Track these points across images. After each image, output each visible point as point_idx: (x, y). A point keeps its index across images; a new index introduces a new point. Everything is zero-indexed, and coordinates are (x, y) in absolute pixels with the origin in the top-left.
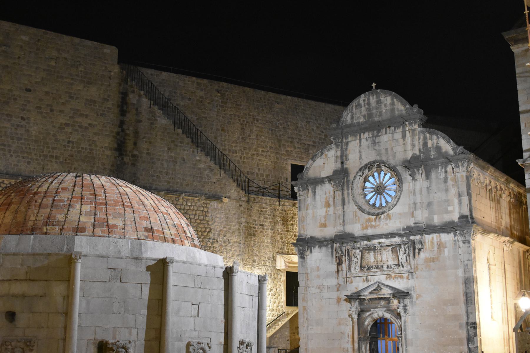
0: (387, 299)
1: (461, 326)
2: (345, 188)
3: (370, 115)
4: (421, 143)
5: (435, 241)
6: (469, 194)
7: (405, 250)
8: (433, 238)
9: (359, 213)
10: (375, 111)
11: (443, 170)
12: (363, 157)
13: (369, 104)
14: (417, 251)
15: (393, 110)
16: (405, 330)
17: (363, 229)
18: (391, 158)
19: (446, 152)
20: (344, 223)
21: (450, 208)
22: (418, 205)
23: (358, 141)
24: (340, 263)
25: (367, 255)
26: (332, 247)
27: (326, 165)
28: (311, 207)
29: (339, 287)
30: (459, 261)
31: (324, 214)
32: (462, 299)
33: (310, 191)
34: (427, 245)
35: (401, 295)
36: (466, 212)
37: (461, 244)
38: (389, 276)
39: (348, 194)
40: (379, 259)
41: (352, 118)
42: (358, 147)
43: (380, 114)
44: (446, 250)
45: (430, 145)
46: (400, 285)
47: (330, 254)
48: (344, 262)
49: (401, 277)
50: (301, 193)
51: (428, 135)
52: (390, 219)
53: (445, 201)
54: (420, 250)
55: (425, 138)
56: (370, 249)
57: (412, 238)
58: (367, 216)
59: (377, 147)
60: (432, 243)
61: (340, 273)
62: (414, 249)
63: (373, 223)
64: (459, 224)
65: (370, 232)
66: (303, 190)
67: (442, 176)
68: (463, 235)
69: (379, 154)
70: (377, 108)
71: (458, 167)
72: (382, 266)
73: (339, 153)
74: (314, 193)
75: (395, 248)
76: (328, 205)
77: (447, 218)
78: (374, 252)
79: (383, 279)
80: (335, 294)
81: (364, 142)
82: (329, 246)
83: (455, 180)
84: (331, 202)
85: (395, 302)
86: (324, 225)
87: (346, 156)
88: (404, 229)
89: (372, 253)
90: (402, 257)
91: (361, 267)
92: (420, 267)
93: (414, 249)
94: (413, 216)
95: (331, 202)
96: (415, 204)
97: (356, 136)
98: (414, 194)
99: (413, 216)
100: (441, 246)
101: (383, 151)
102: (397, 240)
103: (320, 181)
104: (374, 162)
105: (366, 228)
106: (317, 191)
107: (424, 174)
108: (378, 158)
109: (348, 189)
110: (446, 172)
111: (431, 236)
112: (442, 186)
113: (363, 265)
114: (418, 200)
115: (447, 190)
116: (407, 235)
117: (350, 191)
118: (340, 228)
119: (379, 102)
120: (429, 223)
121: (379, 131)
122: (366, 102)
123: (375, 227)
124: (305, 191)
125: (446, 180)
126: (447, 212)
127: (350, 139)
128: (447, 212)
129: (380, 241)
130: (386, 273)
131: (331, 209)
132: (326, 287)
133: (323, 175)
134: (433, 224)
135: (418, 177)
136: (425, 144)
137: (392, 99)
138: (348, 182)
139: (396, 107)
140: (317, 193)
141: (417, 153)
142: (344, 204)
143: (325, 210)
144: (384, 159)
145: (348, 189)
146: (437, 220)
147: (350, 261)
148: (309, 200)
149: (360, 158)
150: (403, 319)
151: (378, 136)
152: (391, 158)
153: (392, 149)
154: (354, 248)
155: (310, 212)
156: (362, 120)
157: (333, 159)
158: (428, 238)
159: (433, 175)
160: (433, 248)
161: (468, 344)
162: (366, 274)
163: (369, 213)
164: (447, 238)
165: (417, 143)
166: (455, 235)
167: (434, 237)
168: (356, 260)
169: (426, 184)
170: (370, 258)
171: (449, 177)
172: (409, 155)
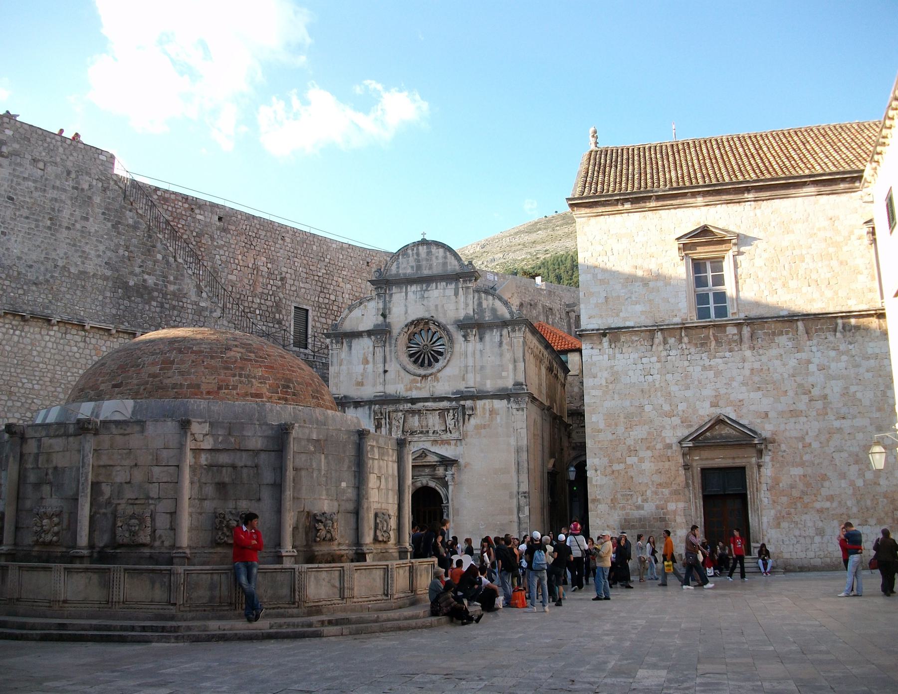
0: (433, 467)
1: (511, 497)
2: (387, 344)
3: (419, 267)
4: (476, 303)
5: (487, 407)
6: (524, 360)
7: (454, 415)
8: (485, 404)
9: (403, 373)
10: (424, 263)
11: (498, 333)
12: (409, 311)
13: (418, 254)
14: (467, 417)
15: (445, 264)
16: (452, 500)
17: (407, 390)
18: (441, 315)
19: (502, 315)
20: (384, 383)
21: (504, 374)
22: (470, 368)
23: (404, 294)
25: (411, 419)
26: (370, 408)
28: (345, 362)
30: (512, 429)
31: (361, 371)
32: (513, 468)
33: (345, 344)
34: (479, 411)
35: (447, 462)
36: (521, 379)
37: (515, 411)
38: (435, 442)
39: (391, 351)
40: (424, 423)
41: (398, 268)
42: (404, 301)
43: (431, 268)
44: (498, 418)
45: (485, 305)
46: (447, 452)
47: (367, 416)
48: (383, 426)
49: (449, 444)
50: (334, 345)
51: (483, 295)
52: (438, 381)
53: (499, 365)
54: (470, 415)
55: (480, 298)
56: (413, 412)
57: (462, 403)
58: (412, 377)
59: (425, 302)
60: (484, 409)
62: (464, 414)
63: (419, 385)
64: (513, 391)
65: (415, 394)
66: (337, 342)
67: (497, 339)
68: (517, 403)
69: (428, 311)
70: (427, 260)
71: (514, 331)
72: (428, 432)
73: (381, 305)
74: (350, 347)
75: (443, 412)
76: (366, 362)
77: (500, 384)
78: (419, 416)
79: (428, 446)
81: (410, 294)
82: (367, 407)
83: (511, 344)
84: (370, 358)
85: (440, 471)
86: (361, 384)
87: (389, 309)
88: (453, 394)
89: (417, 417)
90: (450, 422)
91: (403, 431)
92: (469, 433)
93: (464, 414)
94: (464, 380)
95: (370, 358)
96: (466, 367)
97: (401, 288)
98: (466, 356)
99: (464, 380)
100: (492, 412)
101: (433, 307)
102: (445, 404)
103: (358, 335)
104: (422, 319)
105: (411, 389)
106: (353, 345)
107: (477, 337)
108: (427, 315)
109: (390, 346)
110: (501, 336)
111: (483, 401)
112: (496, 350)
113: (406, 429)
114: (470, 362)
115: (501, 355)
116: (456, 399)
117: (393, 348)
118: (380, 388)
119: (429, 253)
120: (481, 388)
121: (427, 287)
122: (415, 251)
123: (420, 389)
124: (339, 345)
125: (501, 343)
126: (501, 377)
127: (394, 290)
128: (501, 377)
129: (426, 404)
130: (432, 438)
131: (370, 367)
133: (361, 329)
134: (485, 389)
135: (471, 338)
136: (480, 304)
137: (445, 253)
138: (391, 337)
139: (448, 261)
141: (472, 313)
142: (385, 362)
143: (362, 366)
145: (390, 346)
146: (490, 386)
147: (390, 424)
148: (343, 355)
149: (406, 313)
150: (450, 488)
151: (426, 290)
152: (441, 315)
153: (443, 306)
154: (396, 411)
155: (344, 367)
156: (409, 271)
157: (374, 312)
158: (480, 404)
159: (487, 337)
160: (484, 414)
161: (518, 513)
163: (415, 375)
164: (500, 405)
165: (471, 302)
166: (509, 401)
167: (487, 402)
168: (397, 424)
169: (479, 346)
171: (505, 342)
172: (461, 315)
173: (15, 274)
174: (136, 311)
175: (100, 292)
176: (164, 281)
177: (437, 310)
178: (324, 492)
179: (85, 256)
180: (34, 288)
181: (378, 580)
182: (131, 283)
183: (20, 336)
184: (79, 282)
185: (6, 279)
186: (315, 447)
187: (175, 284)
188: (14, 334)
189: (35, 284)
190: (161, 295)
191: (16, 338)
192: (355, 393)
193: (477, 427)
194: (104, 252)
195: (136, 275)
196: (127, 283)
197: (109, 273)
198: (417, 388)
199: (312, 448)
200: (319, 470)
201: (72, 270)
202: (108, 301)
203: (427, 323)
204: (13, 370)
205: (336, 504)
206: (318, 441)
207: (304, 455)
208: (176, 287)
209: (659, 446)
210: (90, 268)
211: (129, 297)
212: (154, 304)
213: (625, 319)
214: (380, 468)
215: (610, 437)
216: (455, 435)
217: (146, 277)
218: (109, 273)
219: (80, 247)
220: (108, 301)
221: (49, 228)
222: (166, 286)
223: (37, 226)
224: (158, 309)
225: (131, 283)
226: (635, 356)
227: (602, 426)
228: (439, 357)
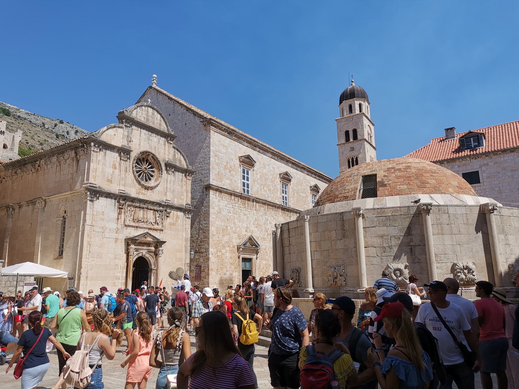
0: (148, 244)
13: (148, 112)
21: (182, 197)
24: (120, 213)
27: (116, 137)
29: (117, 231)
31: (111, 172)
40: (145, 217)
43: (153, 123)
45: (177, 157)
61: (119, 220)
63: (143, 192)
65: (141, 197)
70: (152, 118)
80: (115, 235)
84: (117, 167)
89: (142, 211)
95: (117, 167)
100: (177, 217)
101: (153, 147)
108: (150, 150)
112: (180, 183)
126: (181, 199)
132: (108, 229)
140: (107, 155)
144: (153, 152)
149: (140, 145)
162: (137, 225)
164: (181, 214)
170: (140, 214)
177: (155, 150)
192: (107, 187)
193: (172, 224)
198: (142, 193)
203: (148, 155)
209: (231, 246)
213: (224, 185)
215: (218, 239)
216: (160, 227)
226: (226, 202)
227: (215, 233)
228: (151, 178)
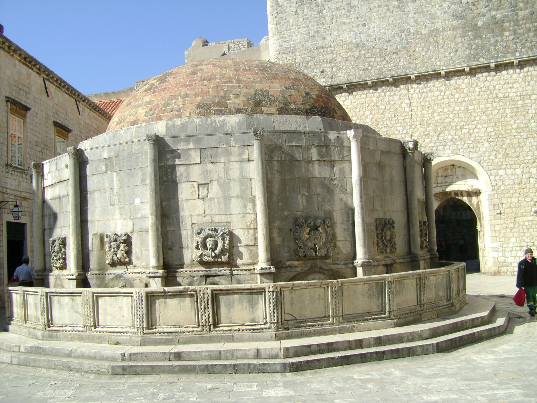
173: (378, 51)
174: (488, 46)
175: (451, 41)
176: (513, 11)
178: (117, 212)
179: (433, 17)
180: (394, 56)
181: (125, 309)
182: (480, 23)
183: (391, 95)
184: (431, 39)
185: (371, 57)
186: (106, 166)
187: (526, 9)
188: (385, 95)
189: (396, 53)
190: (512, 24)
191: (387, 98)
194: (449, 8)
195: (484, 15)
196: (476, 25)
197: (455, 23)
199: (104, 168)
200: (112, 189)
201: (423, 32)
202: (460, 46)
204: (388, 122)
205: (130, 223)
206: (110, 158)
207: (95, 177)
208: (527, 12)
210: (439, 24)
211: (480, 37)
212: (507, 33)
214: (206, 173)
217: (494, 13)
218: (455, 23)
219: (427, 11)
220: (460, 46)
221: (399, 7)
222: (517, 15)
223: (388, 10)
224: (511, 38)
225: (480, 23)
